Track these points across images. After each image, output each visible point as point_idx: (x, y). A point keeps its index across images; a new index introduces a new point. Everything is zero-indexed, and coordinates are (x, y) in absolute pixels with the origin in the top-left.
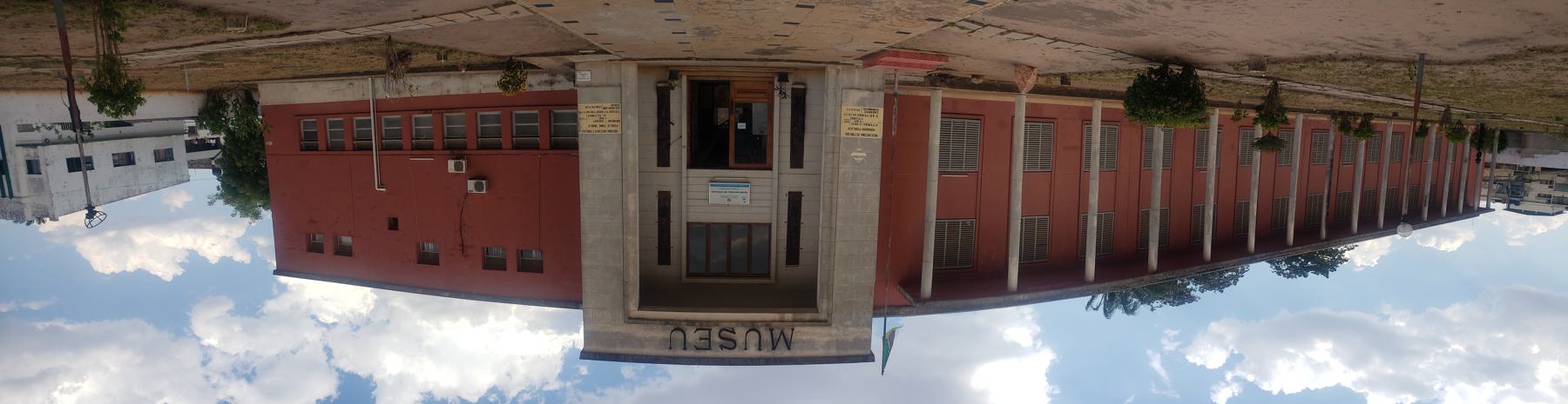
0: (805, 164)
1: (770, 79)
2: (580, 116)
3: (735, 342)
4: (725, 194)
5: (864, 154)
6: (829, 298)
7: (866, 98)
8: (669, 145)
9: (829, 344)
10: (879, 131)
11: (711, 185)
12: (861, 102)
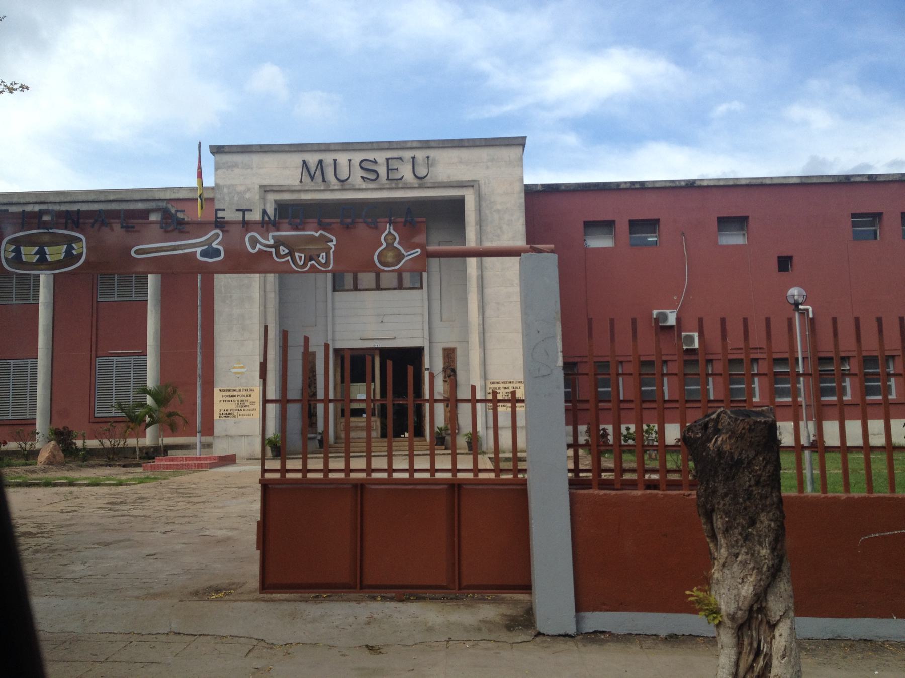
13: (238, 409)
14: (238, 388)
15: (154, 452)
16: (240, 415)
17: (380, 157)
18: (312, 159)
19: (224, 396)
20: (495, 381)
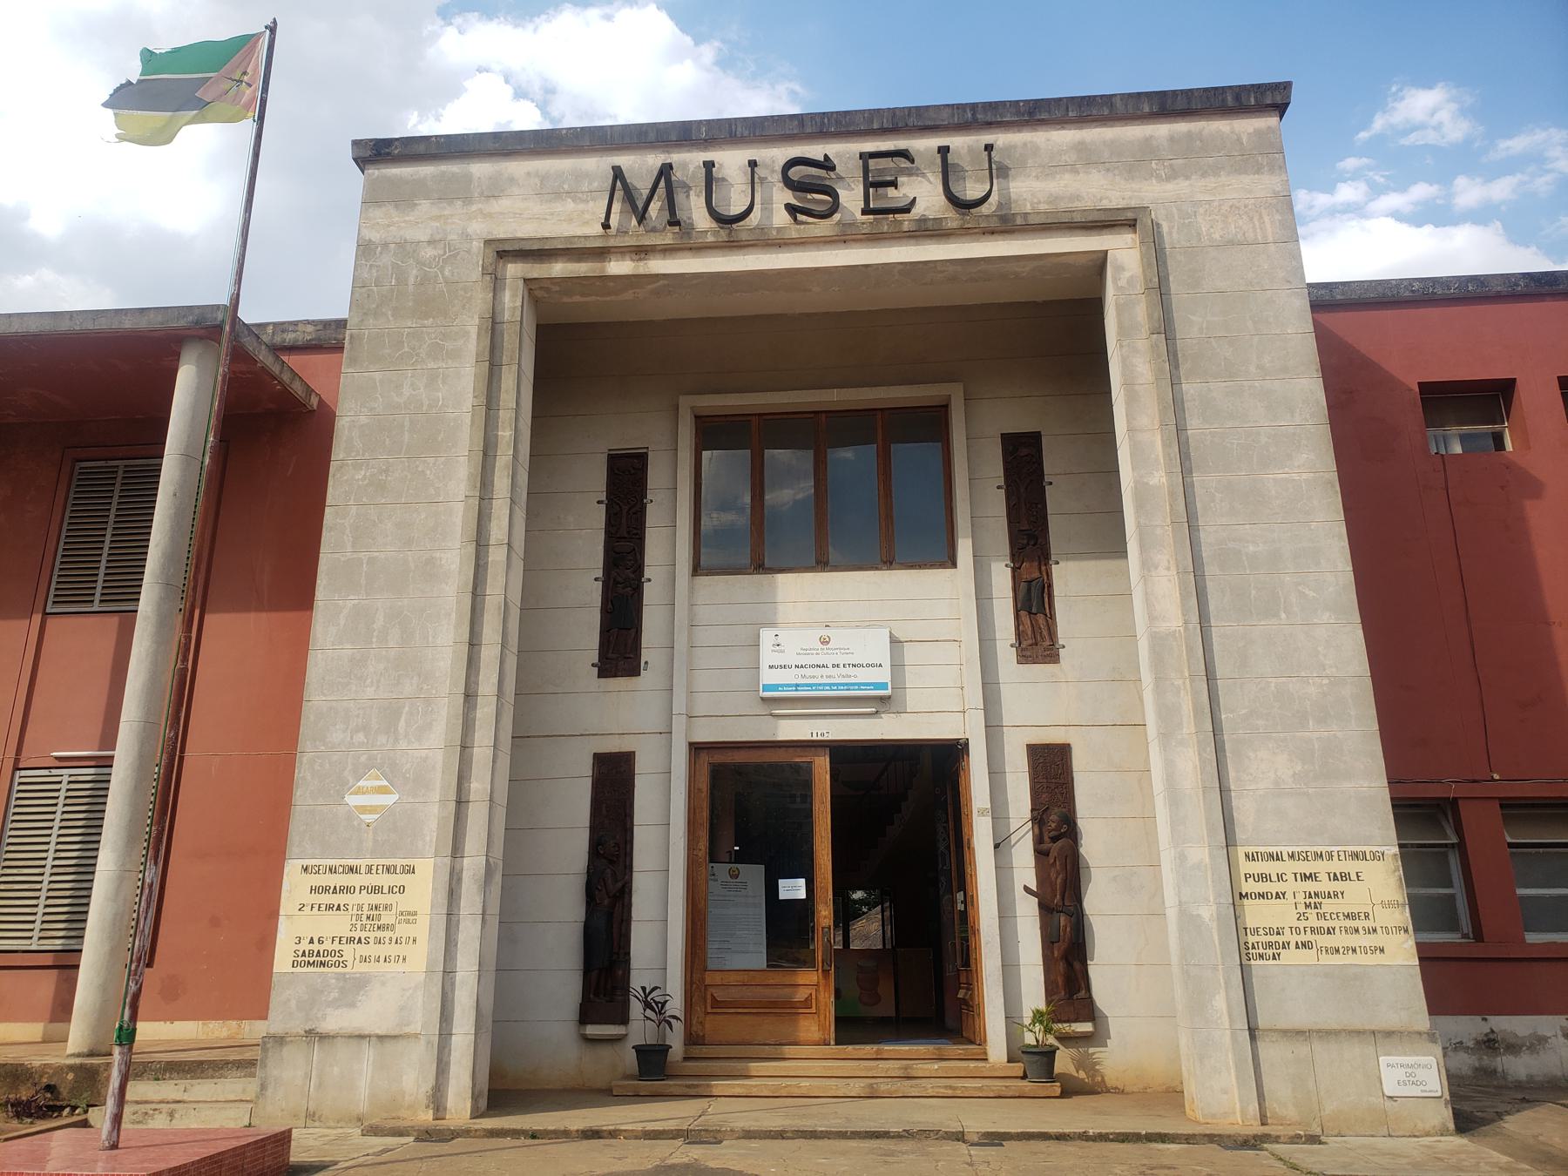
0: (586, 769)
1: (697, 1051)
2: (1403, 917)
3: (789, 183)
4: (841, 660)
5: (352, 800)
6: (494, 326)
7: (336, 1004)
8: (1033, 819)
9: (494, 191)
10: (295, 885)
11: (883, 686)
12: (354, 988)
14: (362, 863)
15: (76, 1089)
16: (365, 960)
17: (844, 152)
18: (641, 165)
19: (314, 890)
20: (1262, 849)
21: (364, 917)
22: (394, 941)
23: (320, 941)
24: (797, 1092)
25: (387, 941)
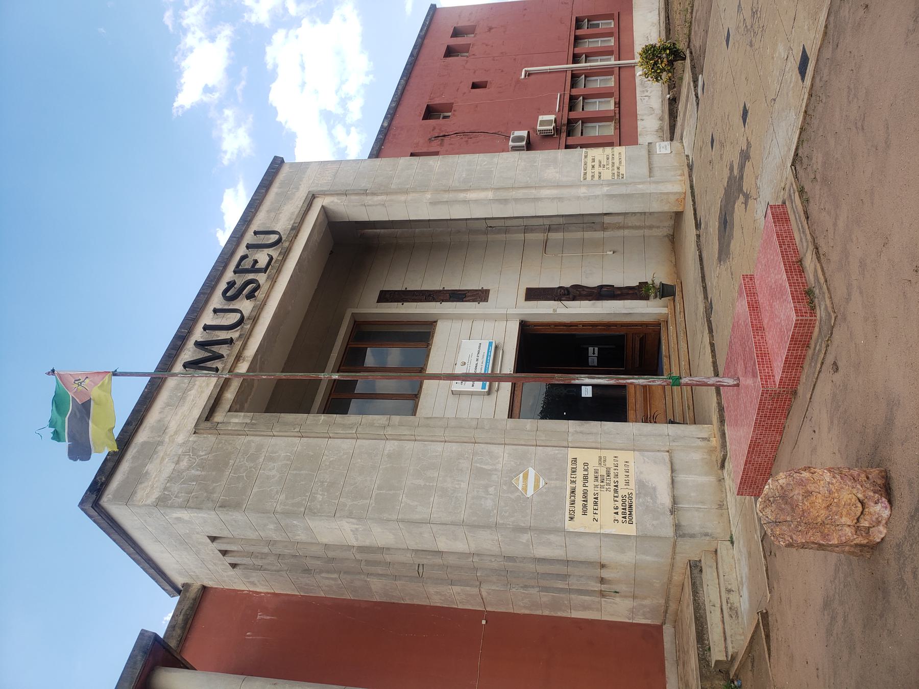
5: (530, 492)
7: (654, 498)
9: (162, 429)
13: (612, 488)
14: (569, 486)
16: (627, 483)
17: (229, 275)
18: (189, 353)
21: (602, 484)
22: (616, 468)
23: (617, 508)
24: (687, 366)
25: (616, 471)
